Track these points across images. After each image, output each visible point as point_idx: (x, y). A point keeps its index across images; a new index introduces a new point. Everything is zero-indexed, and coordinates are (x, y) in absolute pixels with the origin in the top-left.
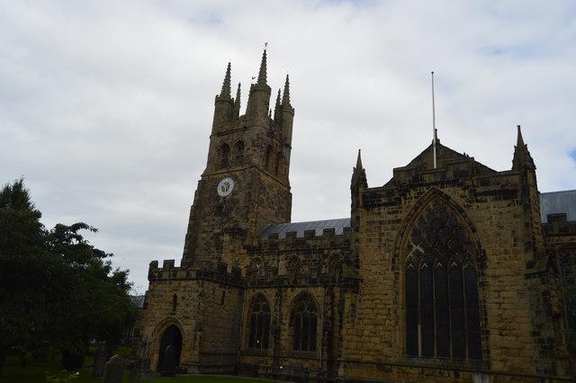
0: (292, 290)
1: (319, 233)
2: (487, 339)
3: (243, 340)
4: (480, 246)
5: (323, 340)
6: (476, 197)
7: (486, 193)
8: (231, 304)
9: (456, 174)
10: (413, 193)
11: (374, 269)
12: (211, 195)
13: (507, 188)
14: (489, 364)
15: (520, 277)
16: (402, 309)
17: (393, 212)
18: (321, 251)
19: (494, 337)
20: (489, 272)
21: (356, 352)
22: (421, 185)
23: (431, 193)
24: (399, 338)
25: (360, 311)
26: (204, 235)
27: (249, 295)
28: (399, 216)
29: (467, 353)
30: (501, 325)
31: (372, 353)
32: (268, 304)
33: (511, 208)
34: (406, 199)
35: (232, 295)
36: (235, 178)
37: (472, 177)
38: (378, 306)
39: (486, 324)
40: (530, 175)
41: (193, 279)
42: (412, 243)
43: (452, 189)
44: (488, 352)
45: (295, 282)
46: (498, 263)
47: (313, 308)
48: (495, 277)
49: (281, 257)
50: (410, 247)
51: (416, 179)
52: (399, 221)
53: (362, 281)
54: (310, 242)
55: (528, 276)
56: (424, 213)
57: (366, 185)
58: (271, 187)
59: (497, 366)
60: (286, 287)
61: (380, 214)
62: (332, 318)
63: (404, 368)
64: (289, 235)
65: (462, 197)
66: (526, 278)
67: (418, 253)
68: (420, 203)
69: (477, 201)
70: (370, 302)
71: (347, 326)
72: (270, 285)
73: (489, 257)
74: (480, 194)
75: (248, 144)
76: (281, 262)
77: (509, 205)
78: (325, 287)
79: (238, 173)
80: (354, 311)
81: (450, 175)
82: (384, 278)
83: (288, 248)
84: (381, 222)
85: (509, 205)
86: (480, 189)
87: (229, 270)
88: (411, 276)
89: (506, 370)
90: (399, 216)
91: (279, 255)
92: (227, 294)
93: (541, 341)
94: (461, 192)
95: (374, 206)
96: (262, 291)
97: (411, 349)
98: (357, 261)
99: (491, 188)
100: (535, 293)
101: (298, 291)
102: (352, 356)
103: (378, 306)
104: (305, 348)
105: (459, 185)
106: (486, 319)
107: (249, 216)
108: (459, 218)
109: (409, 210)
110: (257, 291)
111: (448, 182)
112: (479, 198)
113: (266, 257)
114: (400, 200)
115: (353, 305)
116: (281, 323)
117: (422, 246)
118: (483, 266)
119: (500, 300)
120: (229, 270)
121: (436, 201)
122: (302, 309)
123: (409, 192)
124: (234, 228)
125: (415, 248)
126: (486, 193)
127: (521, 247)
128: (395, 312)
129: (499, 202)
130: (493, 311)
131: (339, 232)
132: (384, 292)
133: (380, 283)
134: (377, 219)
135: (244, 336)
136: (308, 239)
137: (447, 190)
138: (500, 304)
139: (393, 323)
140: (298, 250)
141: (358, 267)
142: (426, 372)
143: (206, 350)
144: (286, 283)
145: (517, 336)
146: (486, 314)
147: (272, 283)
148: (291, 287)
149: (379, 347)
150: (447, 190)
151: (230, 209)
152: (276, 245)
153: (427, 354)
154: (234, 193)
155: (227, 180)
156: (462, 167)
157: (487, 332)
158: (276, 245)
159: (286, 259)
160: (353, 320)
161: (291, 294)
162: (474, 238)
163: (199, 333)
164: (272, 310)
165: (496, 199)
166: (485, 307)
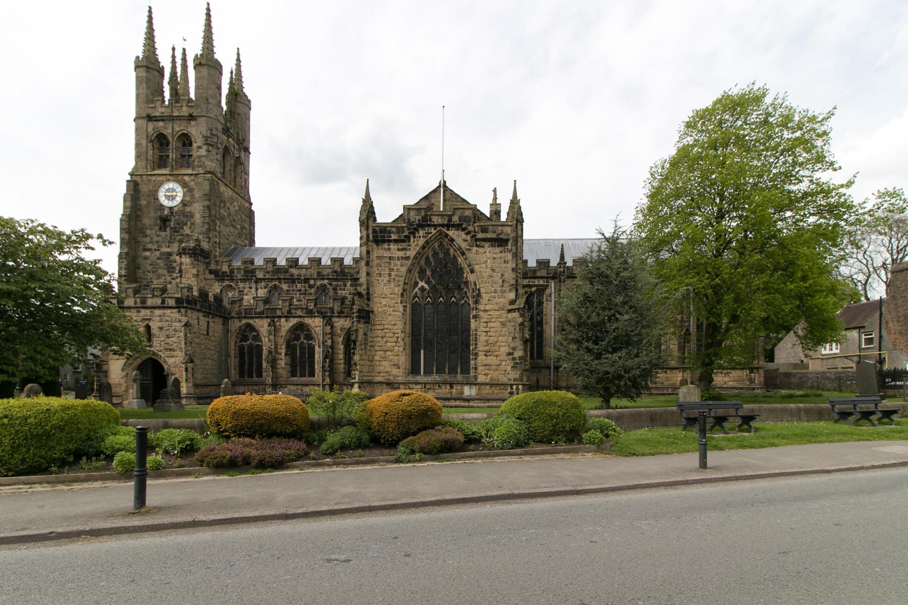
0: (286, 321)
1: (304, 261)
2: (476, 359)
3: (233, 371)
4: (475, 285)
5: (323, 367)
6: (477, 242)
7: (485, 240)
8: (216, 334)
9: (460, 218)
10: (421, 233)
11: (384, 302)
13: (501, 236)
14: (476, 377)
15: (504, 312)
16: (409, 337)
17: (403, 249)
18: (306, 280)
19: (481, 358)
20: (481, 307)
21: (369, 374)
22: (429, 226)
23: (437, 234)
24: (403, 360)
25: (371, 339)
26: (148, 254)
27: (235, 325)
28: (408, 253)
29: (459, 371)
30: (486, 348)
31: (382, 374)
32: (258, 335)
33: (503, 255)
34: (414, 237)
35: (217, 325)
37: (475, 222)
38: (387, 335)
39: (476, 348)
40: (519, 227)
42: (418, 280)
43: (456, 232)
44: (476, 369)
45: (289, 312)
46: (489, 300)
47: (309, 337)
48: (485, 311)
49: (259, 285)
50: (416, 284)
51: (425, 219)
52: (407, 258)
53: (373, 312)
54: (294, 271)
55: (509, 311)
56: (430, 253)
57: (375, 219)
58: (232, 200)
59: (481, 379)
60: (280, 317)
61: (389, 249)
62: (332, 347)
63: (410, 385)
64: (267, 261)
65: (465, 241)
66: (508, 313)
67: (422, 289)
68: (427, 242)
69: (477, 246)
70: (380, 331)
71: (361, 352)
72: (260, 315)
73: (483, 295)
74: (480, 240)
75: (198, 141)
76: (260, 291)
77: (501, 252)
78: (324, 317)
80: (366, 339)
81: (455, 219)
82: (393, 311)
83: (268, 276)
84: (390, 258)
85: (501, 252)
86: (480, 236)
87: (211, 299)
88: (415, 308)
89: (488, 381)
90: (408, 253)
92: (211, 324)
93: (514, 359)
94: (464, 236)
95: (384, 241)
96: (251, 321)
97: (414, 369)
98: (368, 294)
99: (489, 235)
100: (513, 324)
101: (294, 321)
102: (365, 378)
103: (387, 335)
104: (301, 376)
105: (463, 229)
106: (476, 344)
107: (211, 235)
108: (460, 260)
109: (418, 248)
110: (244, 321)
111: (453, 226)
112: (478, 243)
114: (408, 237)
115: (365, 334)
116: (277, 353)
117: (426, 283)
118: (477, 302)
119: (487, 329)
120: (211, 299)
121: (441, 243)
122: (297, 338)
123: (418, 231)
124: (195, 248)
125: (421, 284)
126: (485, 240)
127: (507, 287)
128: (403, 339)
129: (493, 248)
130: (482, 338)
131: (348, 261)
132: (393, 323)
133: (389, 315)
134: (387, 254)
135: (233, 368)
136: (291, 267)
137: (452, 233)
138: (487, 332)
139: (401, 349)
140: (280, 279)
141: (369, 299)
142: (428, 386)
143: (198, 382)
144: (279, 313)
145: (497, 356)
146: (476, 340)
147: (262, 313)
148: (285, 317)
149: (389, 369)
150: (452, 233)
151: (182, 225)
152: (253, 272)
153: (428, 372)
155: (171, 185)
156: (468, 213)
157: (476, 354)
158: (253, 272)
159: (265, 288)
160: (365, 348)
161: (286, 325)
162: (471, 278)
163: (190, 365)
164: (265, 340)
165: (492, 246)
166: (476, 334)
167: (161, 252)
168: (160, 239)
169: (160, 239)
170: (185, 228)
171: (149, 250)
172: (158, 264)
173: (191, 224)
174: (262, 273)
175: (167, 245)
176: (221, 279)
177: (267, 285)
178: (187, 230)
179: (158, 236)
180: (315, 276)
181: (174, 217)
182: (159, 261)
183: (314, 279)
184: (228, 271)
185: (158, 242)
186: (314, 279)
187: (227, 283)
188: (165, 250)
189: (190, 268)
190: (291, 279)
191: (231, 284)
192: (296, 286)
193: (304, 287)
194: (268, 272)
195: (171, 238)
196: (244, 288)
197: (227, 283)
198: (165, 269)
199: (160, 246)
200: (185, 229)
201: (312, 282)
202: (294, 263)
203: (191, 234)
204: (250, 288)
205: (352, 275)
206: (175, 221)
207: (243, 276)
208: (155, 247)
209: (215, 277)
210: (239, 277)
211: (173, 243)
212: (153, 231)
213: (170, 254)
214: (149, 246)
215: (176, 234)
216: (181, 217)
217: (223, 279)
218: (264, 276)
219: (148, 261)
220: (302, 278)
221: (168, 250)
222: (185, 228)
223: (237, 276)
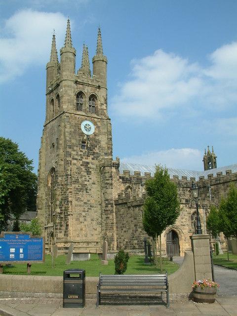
12: (75, 130)
36: (95, 124)
41: (183, 204)
79: (95, 119)
151: (94, 146)
154: (95, 135)
168: (82, 153)
169: (82, 153)
171: (76, 159)
175: (86, 157)
178: (97, 150)
179: (81, 151)
182: (82, 167)
185: (81, 155)
187: (128, 185)
188: (84, 160)
195: (88, 154)
197: (128, 185)
199: (82, 158)
202: (138, 174)
205: (183, 185)
208: (80, 158)
212: (78, 148)
213: (88, 163)
214: (76, 157)
219: (75, 166)
221: (87, 161)
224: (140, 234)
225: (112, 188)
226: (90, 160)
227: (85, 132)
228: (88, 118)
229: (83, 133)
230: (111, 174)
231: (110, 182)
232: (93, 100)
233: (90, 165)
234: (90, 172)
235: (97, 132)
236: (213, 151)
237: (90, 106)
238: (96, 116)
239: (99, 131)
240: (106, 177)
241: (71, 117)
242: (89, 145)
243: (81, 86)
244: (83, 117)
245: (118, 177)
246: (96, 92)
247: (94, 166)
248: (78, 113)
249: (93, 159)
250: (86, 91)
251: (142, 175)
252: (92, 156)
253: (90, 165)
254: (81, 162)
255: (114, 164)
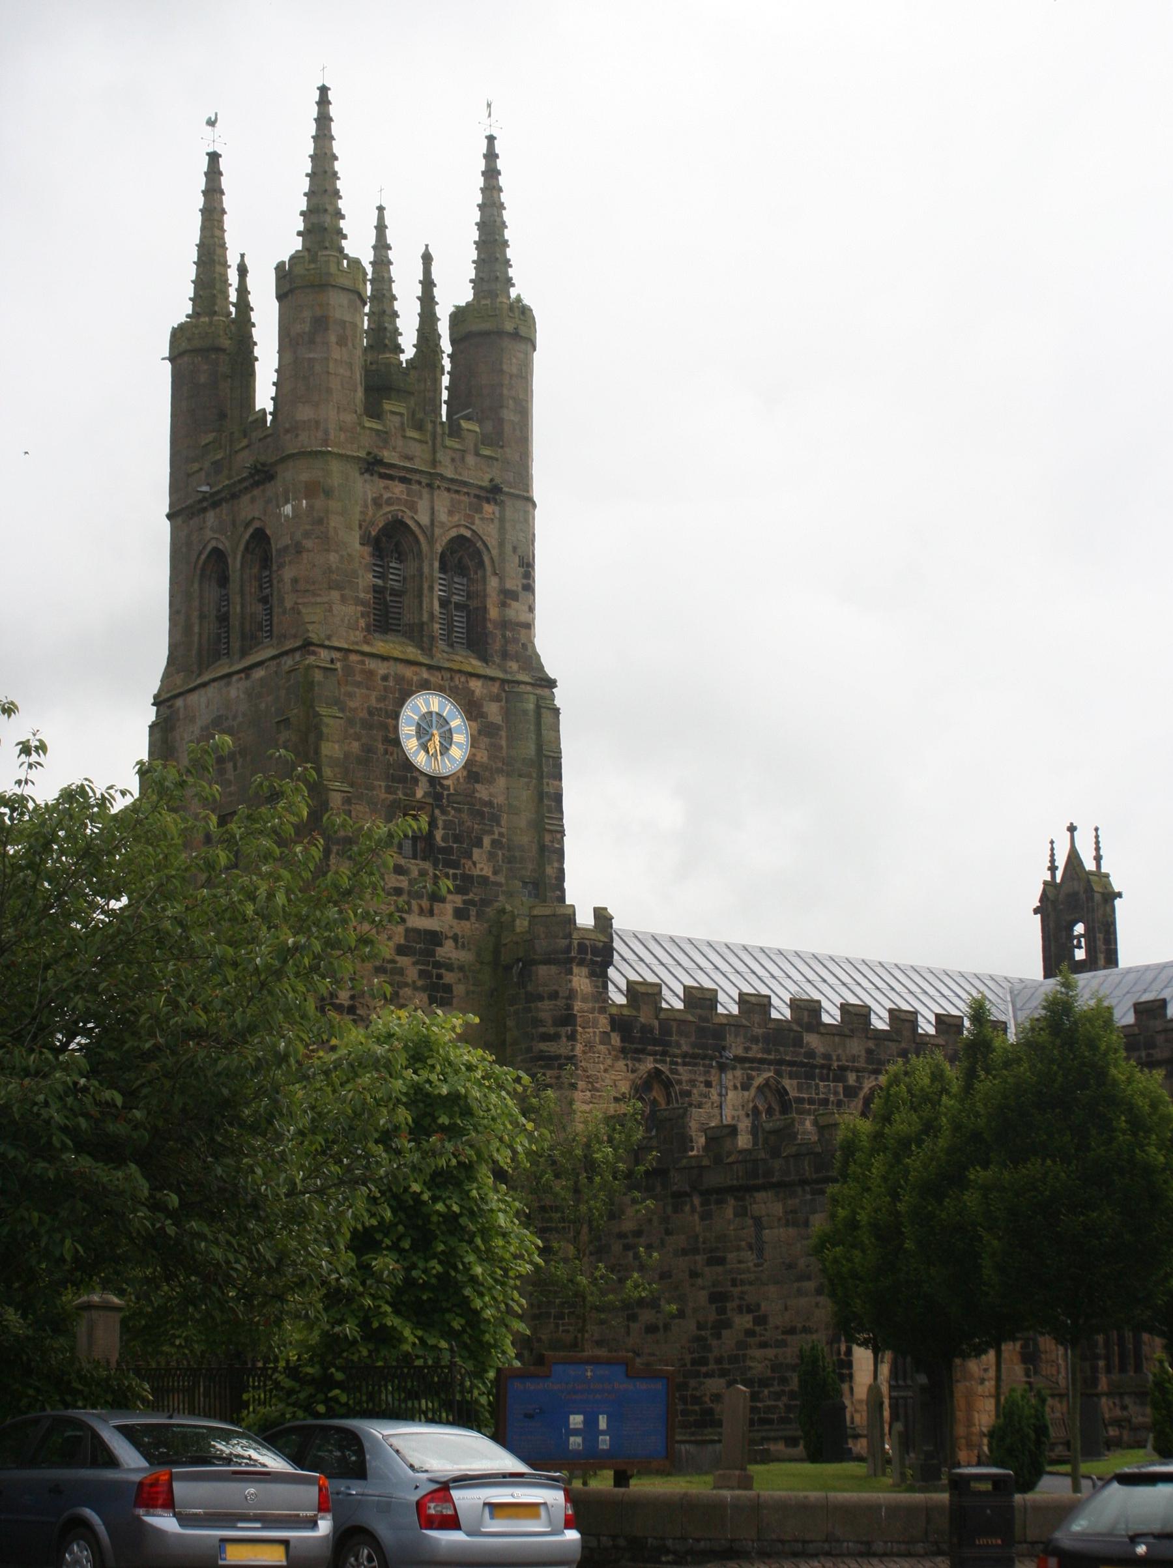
12: (368, 749)
36: (471, 709)
49: (728, 1078)
79: (476, 685)
83: (756, 1052)
91: (722, 1068)
113: (684, 1073)
151: (467, 841)
154: (472, 771)
159: (745, 1087)
167: (407, 930)
168: (404, 883)
170: (476, 852)
172: (401, 972)
173: (494, 843)
174: (740, 1040)
175: (425, 903)
176: (637, 1051)
177: (750, 1078)
178: (481, 864)
180: (861, 1063)
181: (444, 812)
182: (404, 961)
183: (857, 1071)
184: (656, 1023)
185: (398, 891)
186: (857, 1071)
187: (649, 1064)
188: (416, 921)
189: (592, 1011)
190: (803, 1065)
191: (658, 1066)
192: (817, 1086)
193: (836, 1093)
194: (755, 1040)
196: (692, 1082)
198: (424, 989)
200: (475, 857)
201: (851, 1078)
203: (493, 878)
204: (708, 1084)
206: (448, 825)
207: (694, 1046)
209: (622, 1041)
210: (685, 1048)
211: (443, 900)
213: (434, 938)
215: (451, 871)
216: (464, 816)
217: (643, 1051)
218: (747, 1049)
220: (835, 1065)
222: (476, 852)
223: (678, 1045)
224: (742, 1345)
225: (573, 1086)
226: (442, 920)
227: (420, 760)
228: (435, 678)
229: (408, 766)
230: (569, 1007)
231: (560, 1048)
232: (462, 570)
233: (447, 951)
234: (448, 988)
235: (482, 757)
236: (1098, 859)
237: (444, 603)
238: (476, 665)
239: (494, 749)
240: (537, 1022)
241: (349, 670)
242: (439, 835)
243: (398, 489)
244: (408, 672)
245: (603, 1022)
246: (478, 526)
247: (463, 956)
248: (380, 646)
249: (460, 914)
250: (424, 519)
251: (728, 1006)
252: (458, 900)
253: (447, 951)
254: (400, 929)
255: (582, 948)
